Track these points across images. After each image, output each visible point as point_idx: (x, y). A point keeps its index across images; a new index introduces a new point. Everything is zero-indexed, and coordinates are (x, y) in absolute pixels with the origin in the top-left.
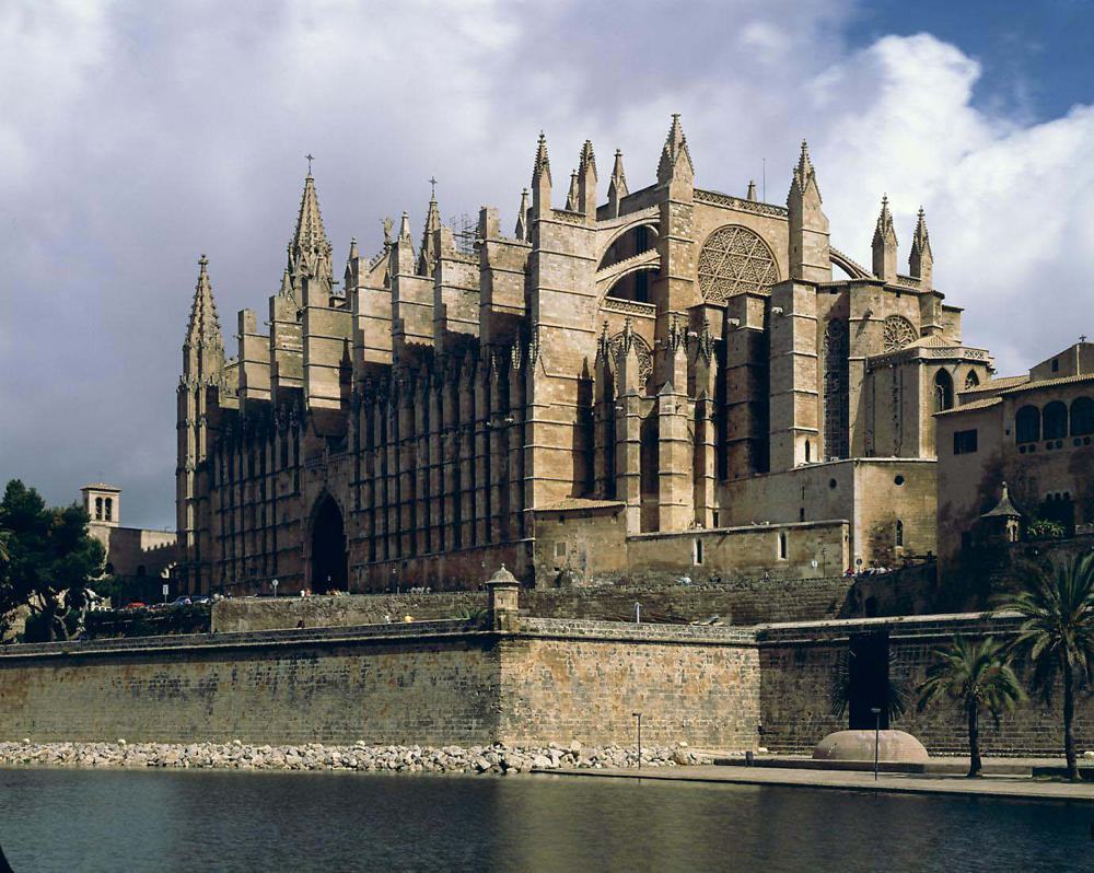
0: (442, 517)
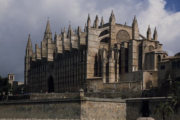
0: (71, 80)
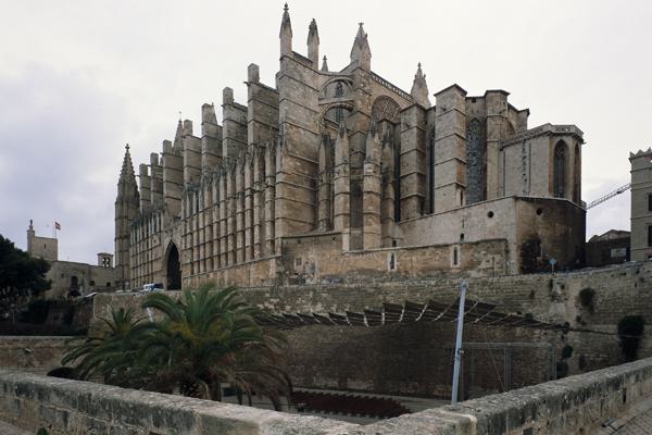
0: (227, 248)
